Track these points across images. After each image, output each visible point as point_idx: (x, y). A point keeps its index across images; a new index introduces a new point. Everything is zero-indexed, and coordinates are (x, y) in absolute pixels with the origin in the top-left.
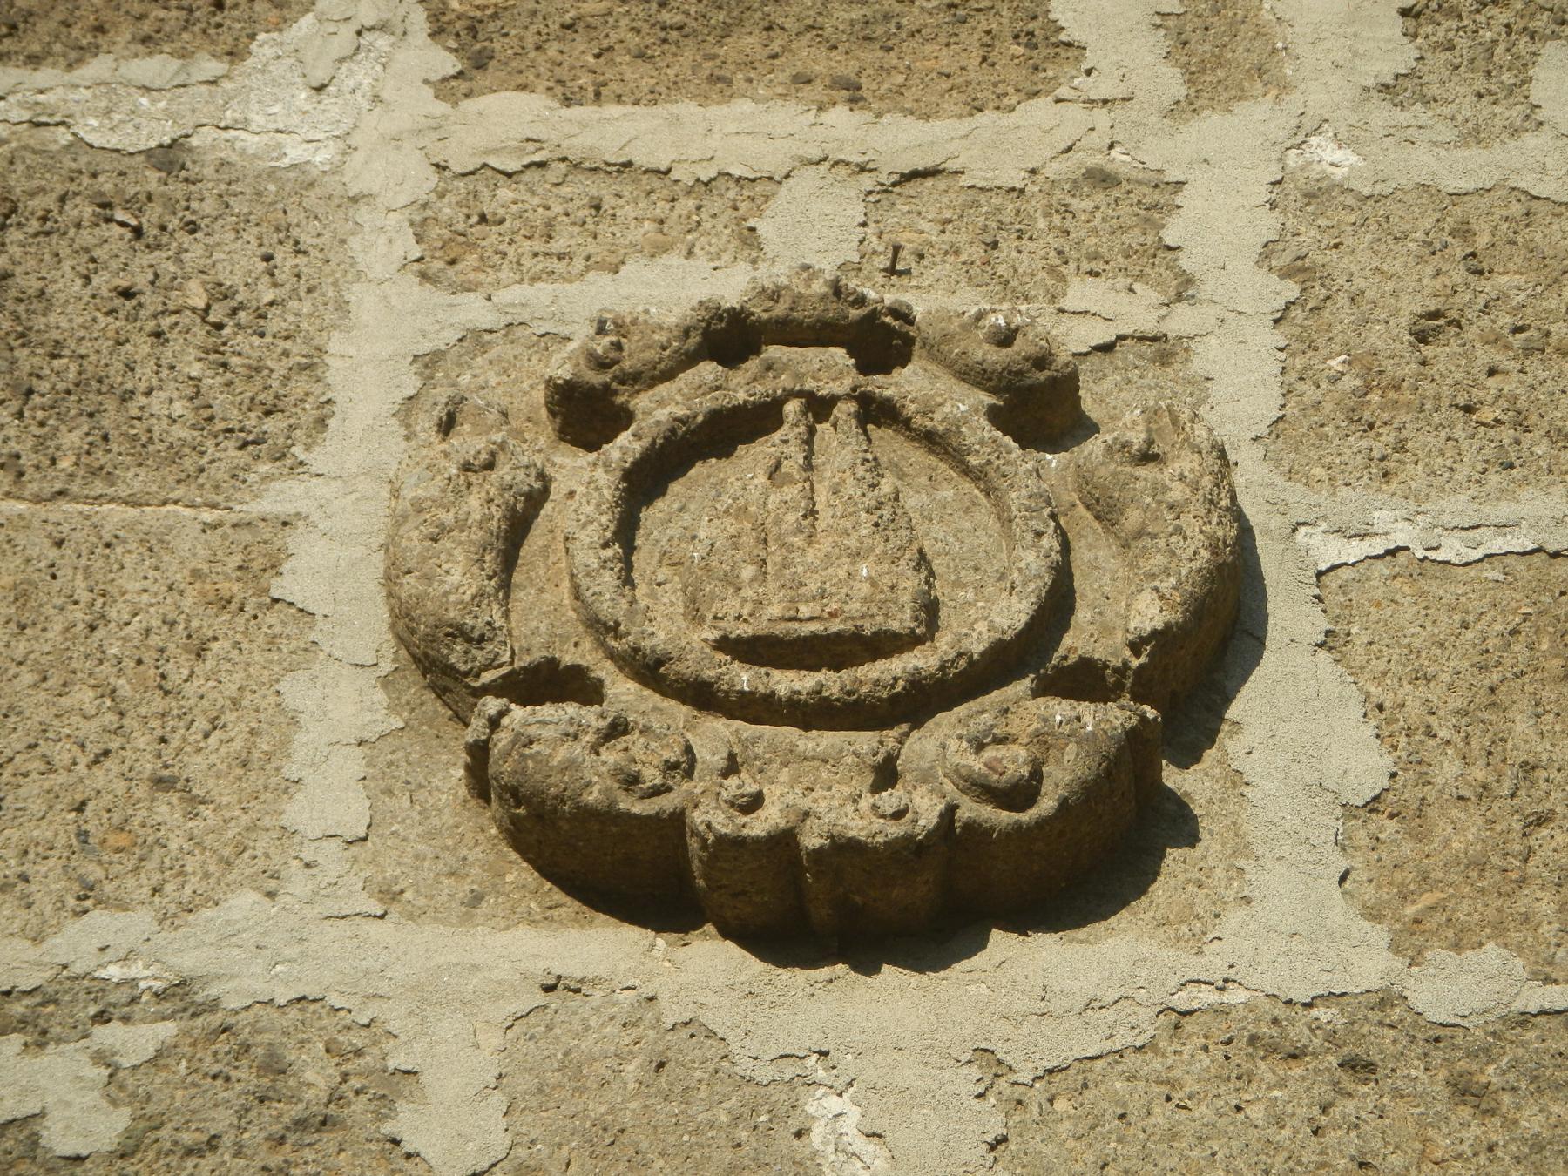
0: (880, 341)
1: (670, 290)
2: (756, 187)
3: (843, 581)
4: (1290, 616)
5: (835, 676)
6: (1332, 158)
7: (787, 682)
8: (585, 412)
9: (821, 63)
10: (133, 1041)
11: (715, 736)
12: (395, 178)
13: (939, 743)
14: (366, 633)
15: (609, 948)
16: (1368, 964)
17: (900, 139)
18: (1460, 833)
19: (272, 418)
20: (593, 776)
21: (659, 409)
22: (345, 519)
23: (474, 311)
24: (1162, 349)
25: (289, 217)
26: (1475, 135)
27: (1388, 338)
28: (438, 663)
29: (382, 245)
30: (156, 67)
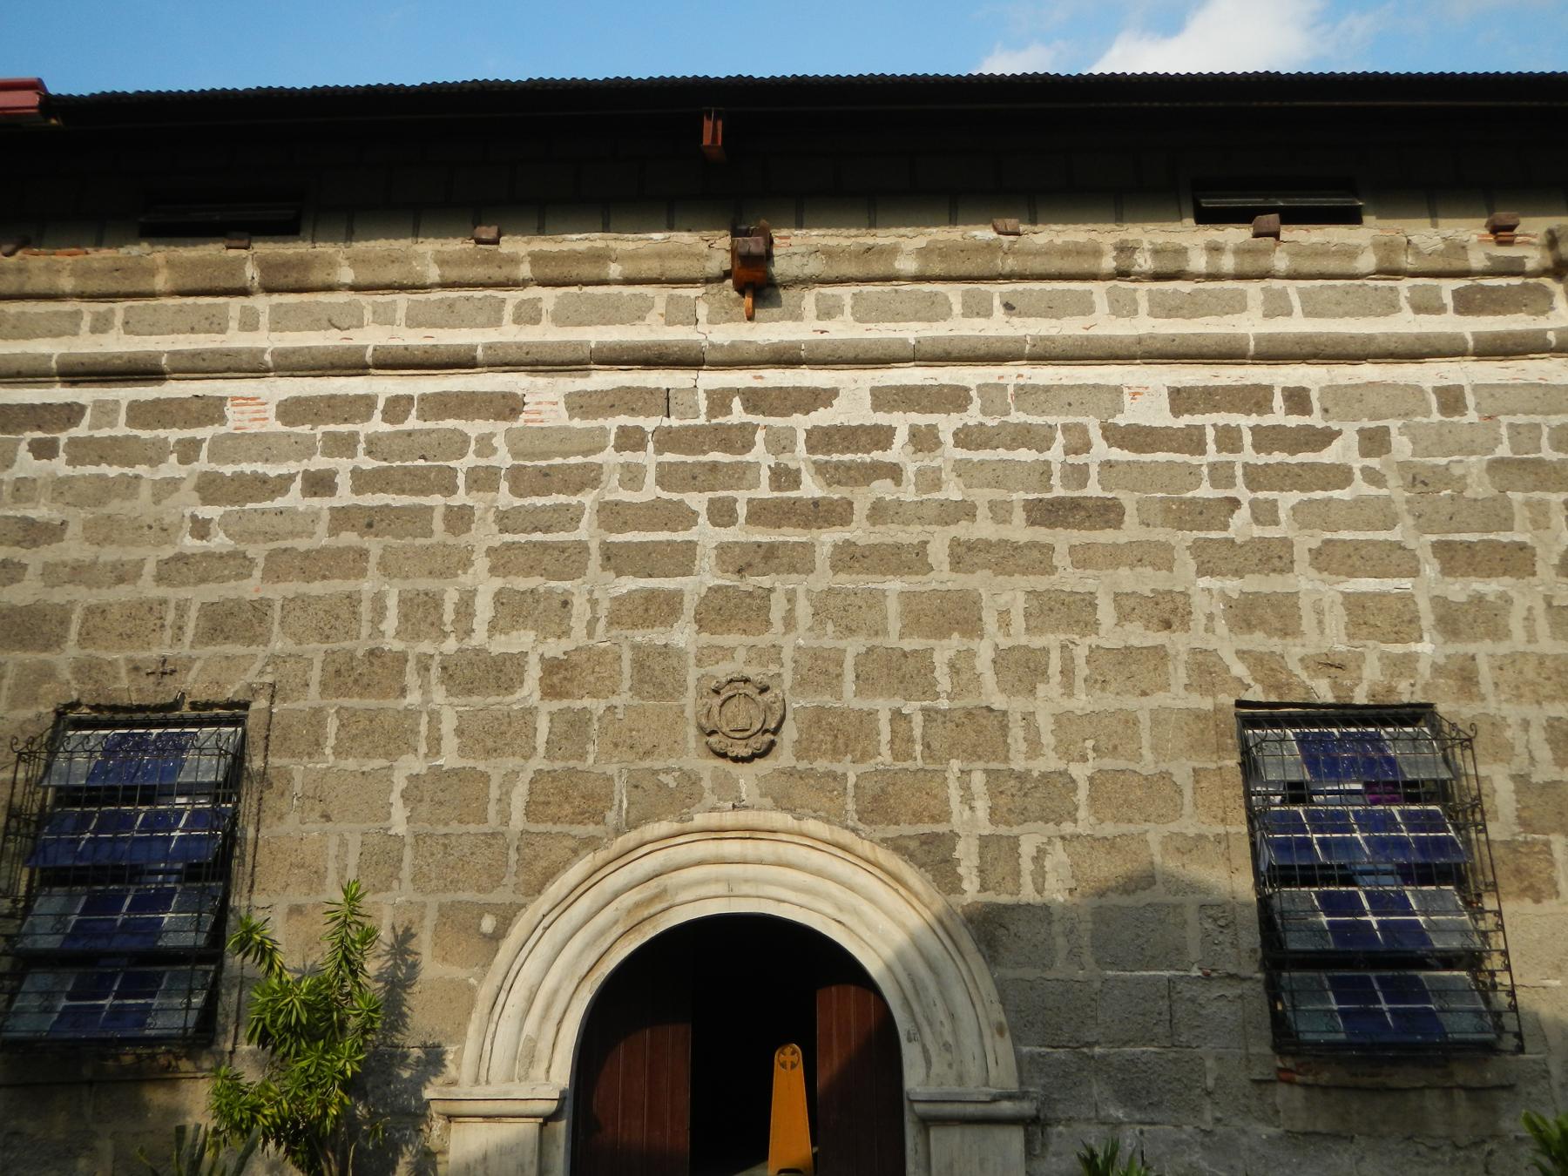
0: (746, 681)
1: (723, 670)
2: (735, 649)
3: (741, 724)
4: (789, 716)
5: (744, 733)
6: (801, 642)
7: (738, 735)
8: (717, 692)
9: (742, 626)
10: (677, 774)
11: (729, 741)
12: (692, 649)
13: (751, 742)
14: (693, 722)
15: (720, 763)
16: (793, 762)
17: (751, 640)
18: (805, 744)
19: (681, 687)
20: (717, 747)
21: (725, 694)
22: (690, 701)
23: (703, 671)
24: (779, 675)
25: (680, 654)
26: (818, 637)
27: (805, 671)
28: (701, 728)
29: (692, 661)
30: (662, 629)
